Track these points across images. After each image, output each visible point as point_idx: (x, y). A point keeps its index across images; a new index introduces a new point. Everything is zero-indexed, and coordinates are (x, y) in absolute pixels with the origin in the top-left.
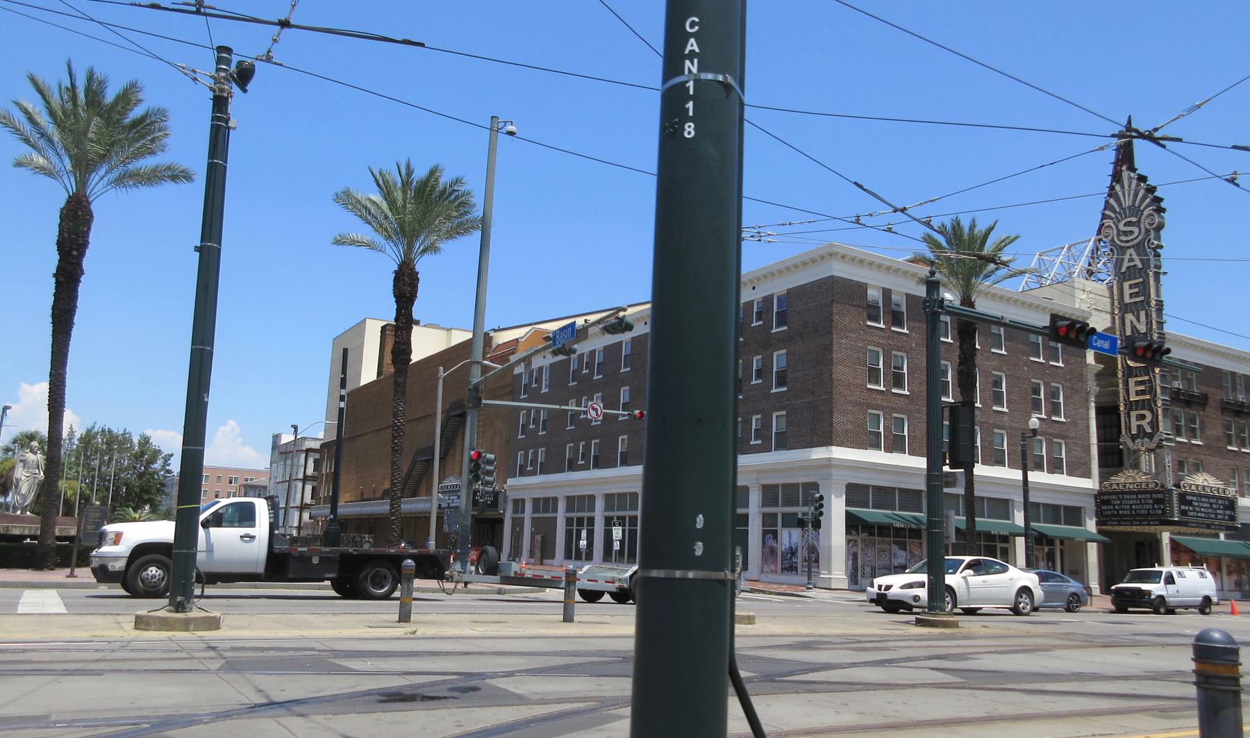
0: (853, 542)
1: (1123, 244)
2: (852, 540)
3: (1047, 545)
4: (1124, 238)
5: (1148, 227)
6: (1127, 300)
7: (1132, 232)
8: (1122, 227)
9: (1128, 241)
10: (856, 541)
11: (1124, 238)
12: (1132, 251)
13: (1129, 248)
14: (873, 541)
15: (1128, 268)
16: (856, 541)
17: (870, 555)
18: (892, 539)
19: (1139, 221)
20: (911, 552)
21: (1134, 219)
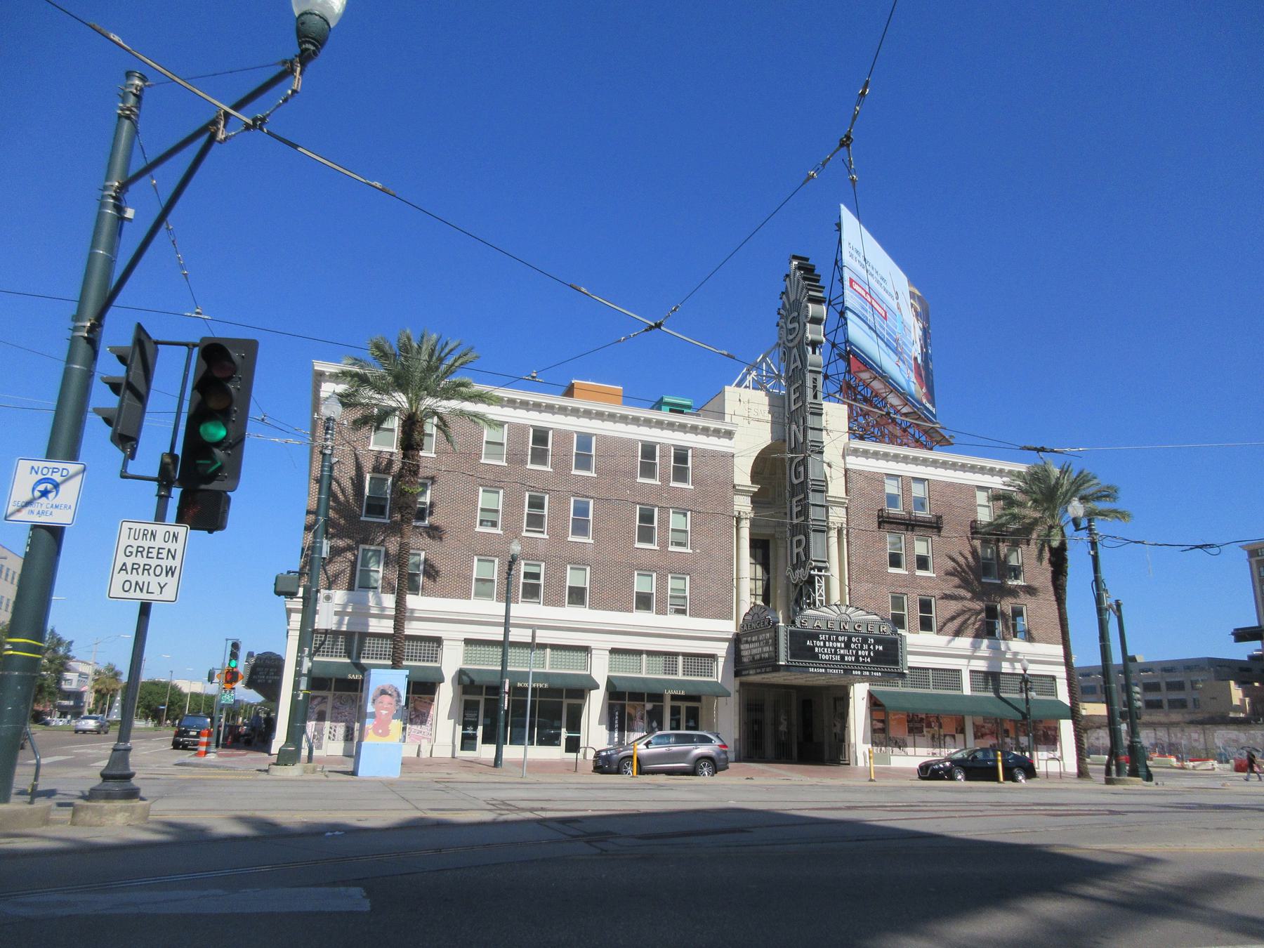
0: (319, 699)
1: (790, 345)
2: (319, 696)
3: (648, 701)
4: (791, 337)
5: (805, 321)
6: (793, 408)
7: (794, 328)
8: (790, 326)
9: (792, 340)
10: (324, 698)
11: (791, 337)
12: (795, 350)
13: (794, 347)
14: (354, 698)
15: (793, 370)
16: (324, 698)
17: (346, 713)
18: (564, 700)
19: (799, 314)
20: (415, 709)
21: (795, 314)
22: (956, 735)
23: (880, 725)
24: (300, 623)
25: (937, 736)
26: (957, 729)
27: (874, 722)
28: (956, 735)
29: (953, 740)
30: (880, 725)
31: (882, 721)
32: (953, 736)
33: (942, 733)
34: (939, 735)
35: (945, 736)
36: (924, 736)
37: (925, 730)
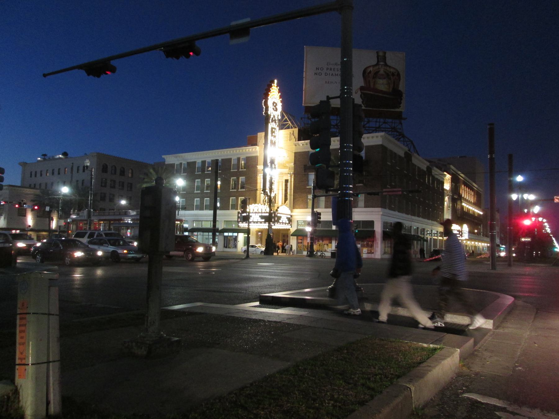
22: (329, 244)
23: (300, 241)
24: (212, 217)
25: (321, 244)
26: (329, 242)
27: (299, 240)
28: (329, 244)
29: (327, 247)
30: (300, 241)
31: (301, 240)
32: (328, 245)
33: (323, 244)
34: (322, 244)
35: (324, 244)
36: (316, 244)
37: (317, 242)
